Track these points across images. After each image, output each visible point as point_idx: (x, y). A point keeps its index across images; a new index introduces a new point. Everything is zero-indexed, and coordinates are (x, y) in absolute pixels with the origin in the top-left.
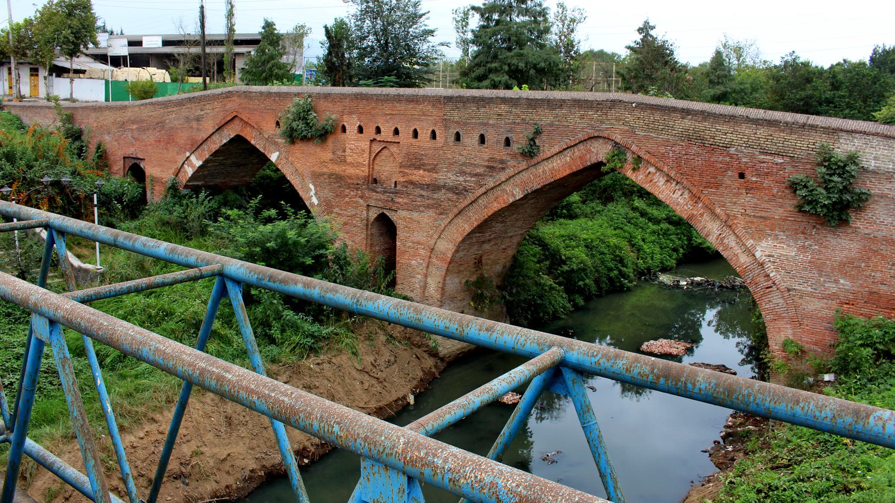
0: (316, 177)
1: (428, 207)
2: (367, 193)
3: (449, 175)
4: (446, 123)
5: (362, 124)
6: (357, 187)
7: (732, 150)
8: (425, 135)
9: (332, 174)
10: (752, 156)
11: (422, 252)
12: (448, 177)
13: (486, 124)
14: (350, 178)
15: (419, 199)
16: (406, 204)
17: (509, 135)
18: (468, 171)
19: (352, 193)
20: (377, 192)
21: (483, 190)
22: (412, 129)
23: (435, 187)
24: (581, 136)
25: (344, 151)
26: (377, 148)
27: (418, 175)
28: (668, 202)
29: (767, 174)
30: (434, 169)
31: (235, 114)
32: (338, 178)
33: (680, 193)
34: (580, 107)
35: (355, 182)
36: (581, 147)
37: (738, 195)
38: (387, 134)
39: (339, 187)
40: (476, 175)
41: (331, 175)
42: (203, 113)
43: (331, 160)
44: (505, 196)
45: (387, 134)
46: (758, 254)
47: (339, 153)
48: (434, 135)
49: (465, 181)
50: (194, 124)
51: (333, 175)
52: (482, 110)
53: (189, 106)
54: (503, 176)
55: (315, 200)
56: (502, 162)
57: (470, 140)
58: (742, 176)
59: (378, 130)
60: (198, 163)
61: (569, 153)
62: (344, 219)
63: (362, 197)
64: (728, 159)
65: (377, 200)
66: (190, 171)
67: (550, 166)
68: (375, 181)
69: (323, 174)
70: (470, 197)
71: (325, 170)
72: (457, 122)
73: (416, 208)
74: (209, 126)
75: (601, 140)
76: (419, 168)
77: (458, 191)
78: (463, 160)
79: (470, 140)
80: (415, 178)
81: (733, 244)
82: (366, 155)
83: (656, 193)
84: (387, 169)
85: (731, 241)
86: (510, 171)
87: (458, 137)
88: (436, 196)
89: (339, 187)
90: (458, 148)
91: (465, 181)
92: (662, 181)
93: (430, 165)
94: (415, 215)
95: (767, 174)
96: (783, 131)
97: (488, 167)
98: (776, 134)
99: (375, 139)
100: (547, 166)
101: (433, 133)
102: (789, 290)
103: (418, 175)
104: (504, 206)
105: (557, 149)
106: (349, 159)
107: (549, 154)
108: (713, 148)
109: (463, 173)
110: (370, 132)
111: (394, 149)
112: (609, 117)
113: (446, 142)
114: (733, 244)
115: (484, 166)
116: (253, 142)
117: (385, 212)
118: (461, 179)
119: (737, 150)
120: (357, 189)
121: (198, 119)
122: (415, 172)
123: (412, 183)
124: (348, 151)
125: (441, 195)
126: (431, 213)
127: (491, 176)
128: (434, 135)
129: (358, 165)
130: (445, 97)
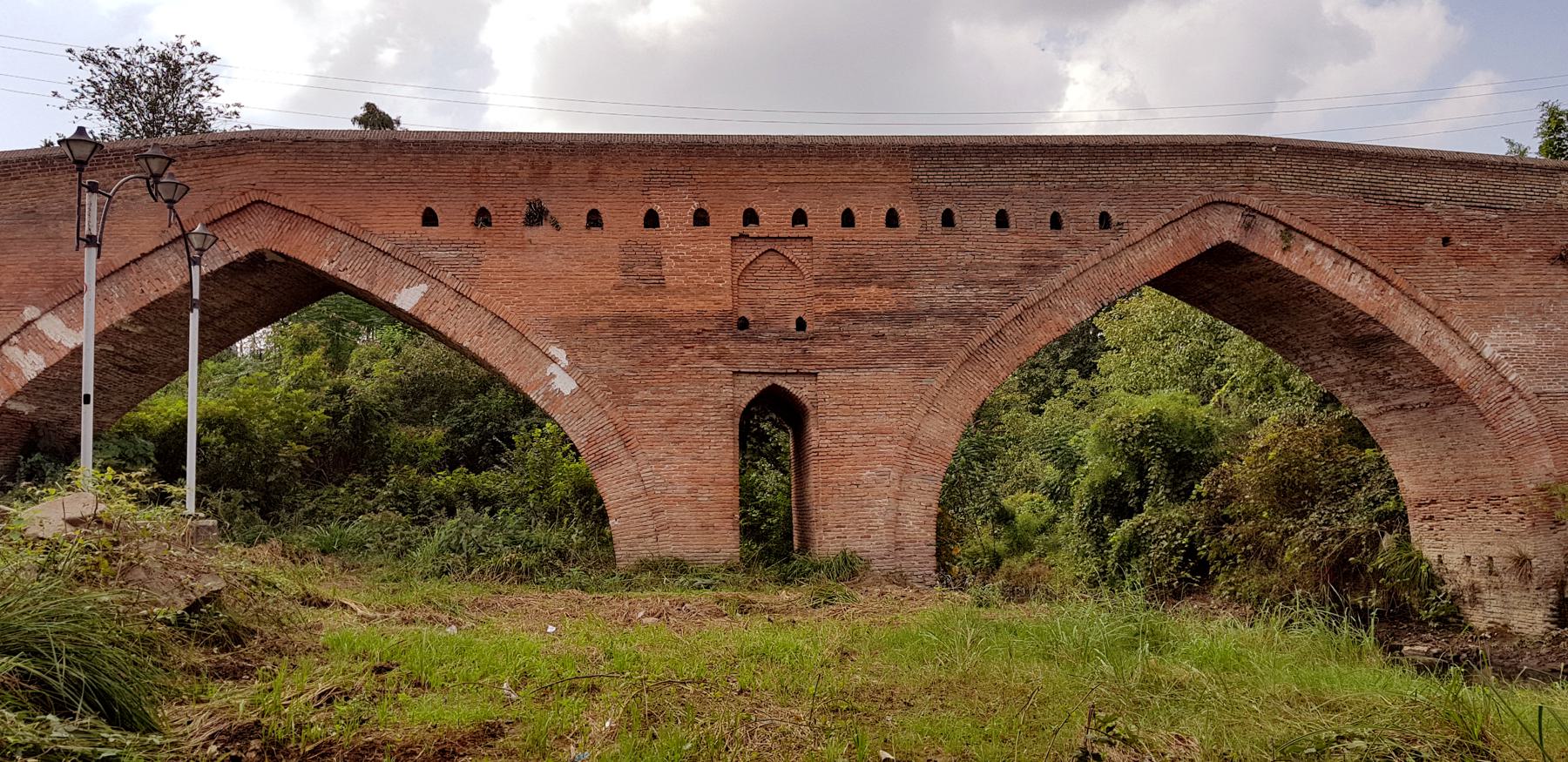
0: (572, 330)
1: (898, 355)
2: (731, 347)
3: (940, 289)
5: (705, 206)
6: (701, 337)
7: (1429, 207)
10: (1457, 214)
11: (889, 450)
14: (679, 319)
16: (839, 356)
17: (1059, 209)
18: (981, 277)
19: (688, 352)
20: (758, 341)
21: (1016, 310)
22: (842, 209)
23: (909, 317)
24: (1191, 203)
25: (659, 265)
27: (866, 297)
28: (1343, 295)
29: (1480, 236)
30: (902, 280)
31: (254, 196)
33: (1358, 278)
34: (1185, 155)
35: (695, 327)
36: (1190, 221)
37: (1446, 269)
38: (774, 219)
41: (618, 322)
43: (615, 287)
44: (1060, 318)
45: (774, 219)
46: (1487, 352)
48: (892, 219)
49: (978, 297)
52: (997, 168)
53: (41, 180)
54: (1056, 280)
55: (565, 384)
56: (1051, 255)
57: (978, 222)
58: (1446, 241)
59: (751, 217)
61: (1170, 232)
62: (666, 413)
63: (718, 358)
64: (1424, 220)
67: (1140, 256)
68: (743, 324)
70: (992, 327)
71: (598, 311)
73: (869, 363)
75: (1222, 208)
76: (868, 283)
77: (965, 317)
78: (968, 258)
79: (978, 222)
81: (1446, 344)
82: (724, 268)
83: (1323, 283)
85: (1443, 339)
86: (1070, 271)
87: (948, 219)
88: (912, 332)
90: (951, 238)
91: (978, 297)
92: (1329, 263)
93: (888, 273)
94: (865, 376)
95: (1480, 236)
97: (1023, 267)
99: (742, 236)
100: (1135, 257)
102: (1538, 395)
103: (866, 297)
104: (1058, 334)
105: (1151, 226)
106: (671, 282)
107: (1138, 235)
108: (1402, 206)
109: (970, 283)
110: (728, 219)
111: (794, 252)
112: (1236, 170)
113: (925, 228)
114: (1446, 344)
115: (1016, 266)
117: (779, 381)
118: (968, 293)
120: (703, 342)
122: (857, 291)
123: (854, 314)
126: (907, 365)
127: (1033, 282)
128: (892, 219)
129: (703, 290)
130: (912, 148)
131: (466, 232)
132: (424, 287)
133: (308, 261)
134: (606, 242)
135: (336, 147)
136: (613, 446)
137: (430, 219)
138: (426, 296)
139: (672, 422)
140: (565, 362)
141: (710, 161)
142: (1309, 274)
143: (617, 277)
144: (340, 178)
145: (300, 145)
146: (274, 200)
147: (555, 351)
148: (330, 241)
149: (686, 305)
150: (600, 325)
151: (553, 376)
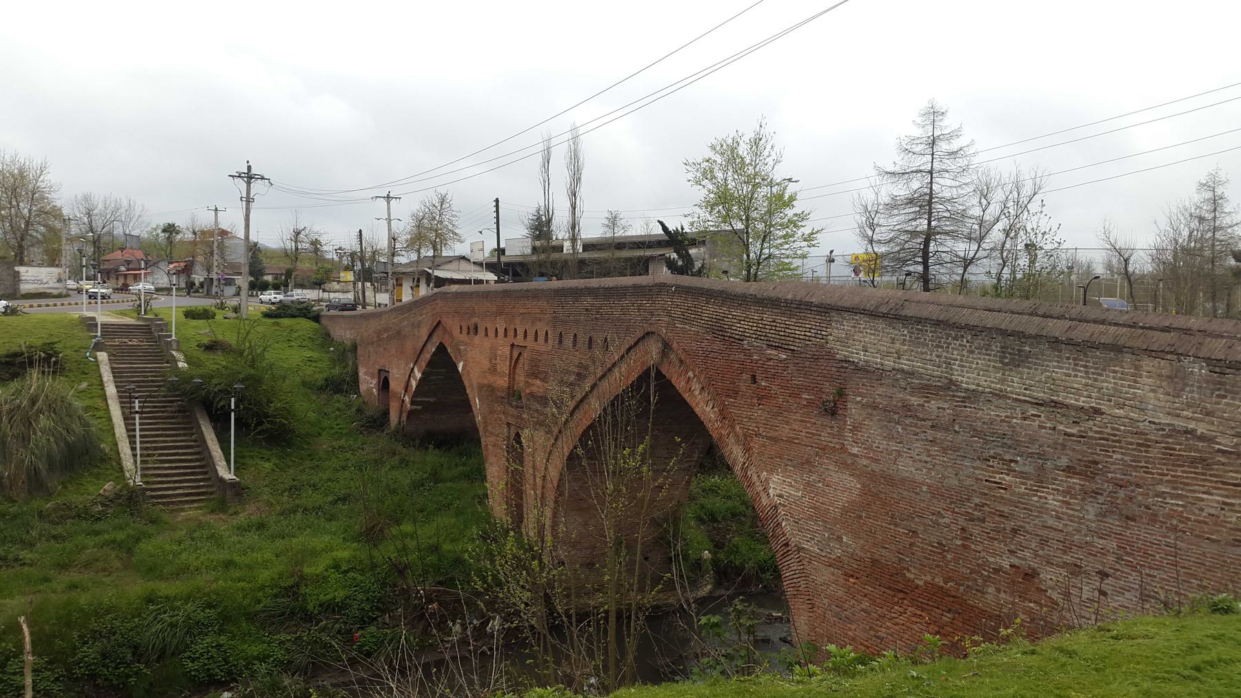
9: (489, 386)
10: (760, 351)
12: (553, 388)
13: (577, 322)
24: (639, 334)
26: (515, 355)
32: (491, 389)
56: (586, 368)
57: (568, 342)
60: (418, 375)
66: (414, 384)
74: (424, 332)
76: (536, 377)
79: (568, 342)
80: (534, 389)
96: (783, 314)
97: (579, 374)
98: (780, 319)
103: (537, 386)
110: (511, 333)
119: (749, 344)
134: (487, 343)
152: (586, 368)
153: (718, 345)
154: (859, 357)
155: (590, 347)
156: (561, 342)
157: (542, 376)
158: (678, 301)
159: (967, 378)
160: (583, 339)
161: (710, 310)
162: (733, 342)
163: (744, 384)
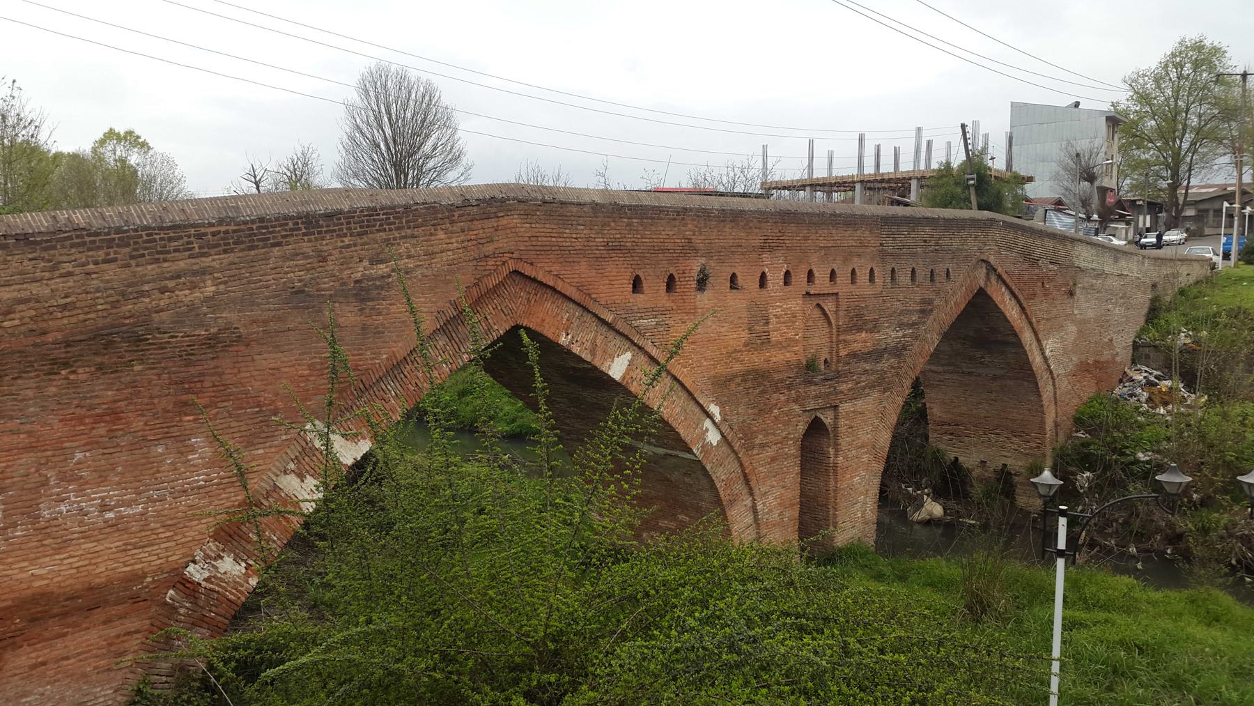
0: (722, 386)
1: (872, 387)
4: (883, 256)
8: (863, 277)
12: (890, 335)
13: (914, 255)
15: (863, 378)
20: (816, 384)
23: (876, 354)
30: (875, 329)
31: (512, 265)
32: (759, 379)
39: (763, 392)
40: (913, 325)
41: (745, 376)
42: (382, 269)
43: (746, 345)
47: (758, 328)
49: (904, 336)
50: (348, 315)
51: (748, 372)
56: (930, 302)
57: (904, 278)
59: (810, 274)
62: (770, 452)
63: (796, 401)
65: (816, 397)
69: (732, 378)
71: (737, 367)
72: (892, 255)
76: (860, 330)
79: (904, 278)
80: (856, 346)
84: (816, 341)
89: (763, 392)
94: (859, 402)
97: (922, 311)
101: (872, 270)
103: (862, 341)
106: (774, 337)
110: (800, 278)
116: (563, 340)
117: (819, 415)
118: (900, 334)
120: (789, 388)
121: (363, 293)
124: (773, 320)
125: (885, 364)
126: (876, 395)
131: (663, 300)
132: (628, 355)
133: (550, 335)
134: (737, 302)
135: (575, 209)
136: (740, 486)
137: (637, 285)
138: (631, 362)
139: (773, 459)
140: (718, 418)
141: (793, 227)
142: (1001, 307)
143: (745, 335)
144: (578, 245)
145: (547, 207)
146: (528, 270)
147: (715, 410)
148: (568, 312)
149: (779, 357)
150: (738, 380)
151: (707, 430)
152: (930, 302)
153: (1026, 265)
154: (1082, 265)
155: (932, 280)
156: (893, 279)
157: (870, 325)
158: (1004, 233)
159: (1108, 269)
160: (922, 273)
161: (1023, 240)
162: (1034, 262)
163: (1039, 290)
